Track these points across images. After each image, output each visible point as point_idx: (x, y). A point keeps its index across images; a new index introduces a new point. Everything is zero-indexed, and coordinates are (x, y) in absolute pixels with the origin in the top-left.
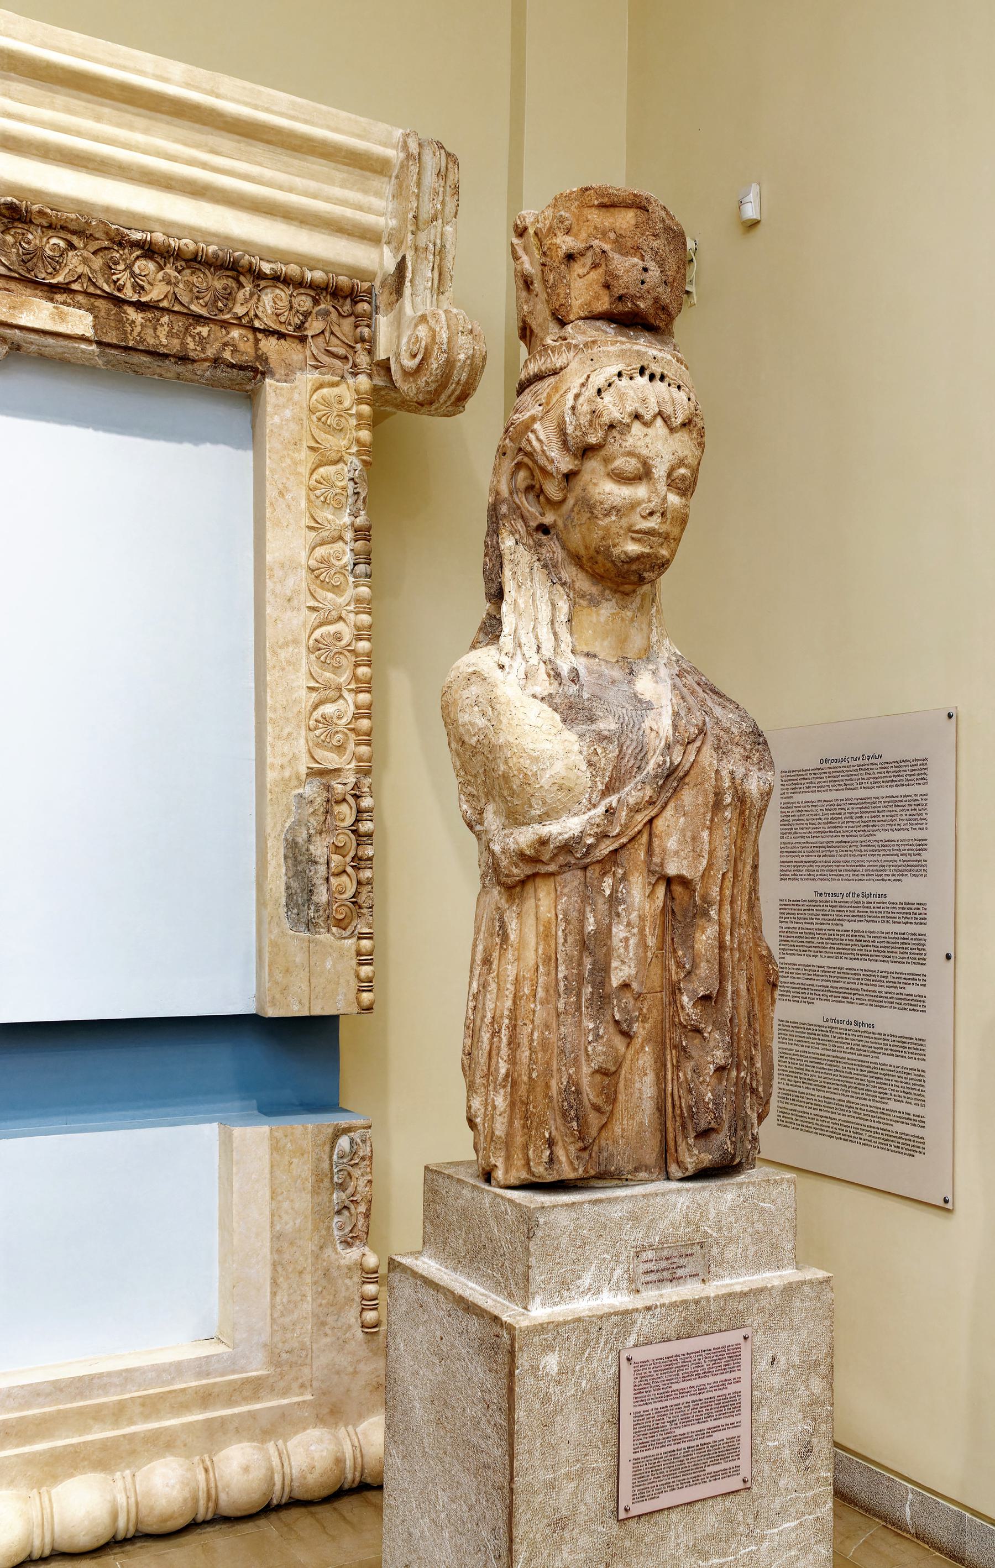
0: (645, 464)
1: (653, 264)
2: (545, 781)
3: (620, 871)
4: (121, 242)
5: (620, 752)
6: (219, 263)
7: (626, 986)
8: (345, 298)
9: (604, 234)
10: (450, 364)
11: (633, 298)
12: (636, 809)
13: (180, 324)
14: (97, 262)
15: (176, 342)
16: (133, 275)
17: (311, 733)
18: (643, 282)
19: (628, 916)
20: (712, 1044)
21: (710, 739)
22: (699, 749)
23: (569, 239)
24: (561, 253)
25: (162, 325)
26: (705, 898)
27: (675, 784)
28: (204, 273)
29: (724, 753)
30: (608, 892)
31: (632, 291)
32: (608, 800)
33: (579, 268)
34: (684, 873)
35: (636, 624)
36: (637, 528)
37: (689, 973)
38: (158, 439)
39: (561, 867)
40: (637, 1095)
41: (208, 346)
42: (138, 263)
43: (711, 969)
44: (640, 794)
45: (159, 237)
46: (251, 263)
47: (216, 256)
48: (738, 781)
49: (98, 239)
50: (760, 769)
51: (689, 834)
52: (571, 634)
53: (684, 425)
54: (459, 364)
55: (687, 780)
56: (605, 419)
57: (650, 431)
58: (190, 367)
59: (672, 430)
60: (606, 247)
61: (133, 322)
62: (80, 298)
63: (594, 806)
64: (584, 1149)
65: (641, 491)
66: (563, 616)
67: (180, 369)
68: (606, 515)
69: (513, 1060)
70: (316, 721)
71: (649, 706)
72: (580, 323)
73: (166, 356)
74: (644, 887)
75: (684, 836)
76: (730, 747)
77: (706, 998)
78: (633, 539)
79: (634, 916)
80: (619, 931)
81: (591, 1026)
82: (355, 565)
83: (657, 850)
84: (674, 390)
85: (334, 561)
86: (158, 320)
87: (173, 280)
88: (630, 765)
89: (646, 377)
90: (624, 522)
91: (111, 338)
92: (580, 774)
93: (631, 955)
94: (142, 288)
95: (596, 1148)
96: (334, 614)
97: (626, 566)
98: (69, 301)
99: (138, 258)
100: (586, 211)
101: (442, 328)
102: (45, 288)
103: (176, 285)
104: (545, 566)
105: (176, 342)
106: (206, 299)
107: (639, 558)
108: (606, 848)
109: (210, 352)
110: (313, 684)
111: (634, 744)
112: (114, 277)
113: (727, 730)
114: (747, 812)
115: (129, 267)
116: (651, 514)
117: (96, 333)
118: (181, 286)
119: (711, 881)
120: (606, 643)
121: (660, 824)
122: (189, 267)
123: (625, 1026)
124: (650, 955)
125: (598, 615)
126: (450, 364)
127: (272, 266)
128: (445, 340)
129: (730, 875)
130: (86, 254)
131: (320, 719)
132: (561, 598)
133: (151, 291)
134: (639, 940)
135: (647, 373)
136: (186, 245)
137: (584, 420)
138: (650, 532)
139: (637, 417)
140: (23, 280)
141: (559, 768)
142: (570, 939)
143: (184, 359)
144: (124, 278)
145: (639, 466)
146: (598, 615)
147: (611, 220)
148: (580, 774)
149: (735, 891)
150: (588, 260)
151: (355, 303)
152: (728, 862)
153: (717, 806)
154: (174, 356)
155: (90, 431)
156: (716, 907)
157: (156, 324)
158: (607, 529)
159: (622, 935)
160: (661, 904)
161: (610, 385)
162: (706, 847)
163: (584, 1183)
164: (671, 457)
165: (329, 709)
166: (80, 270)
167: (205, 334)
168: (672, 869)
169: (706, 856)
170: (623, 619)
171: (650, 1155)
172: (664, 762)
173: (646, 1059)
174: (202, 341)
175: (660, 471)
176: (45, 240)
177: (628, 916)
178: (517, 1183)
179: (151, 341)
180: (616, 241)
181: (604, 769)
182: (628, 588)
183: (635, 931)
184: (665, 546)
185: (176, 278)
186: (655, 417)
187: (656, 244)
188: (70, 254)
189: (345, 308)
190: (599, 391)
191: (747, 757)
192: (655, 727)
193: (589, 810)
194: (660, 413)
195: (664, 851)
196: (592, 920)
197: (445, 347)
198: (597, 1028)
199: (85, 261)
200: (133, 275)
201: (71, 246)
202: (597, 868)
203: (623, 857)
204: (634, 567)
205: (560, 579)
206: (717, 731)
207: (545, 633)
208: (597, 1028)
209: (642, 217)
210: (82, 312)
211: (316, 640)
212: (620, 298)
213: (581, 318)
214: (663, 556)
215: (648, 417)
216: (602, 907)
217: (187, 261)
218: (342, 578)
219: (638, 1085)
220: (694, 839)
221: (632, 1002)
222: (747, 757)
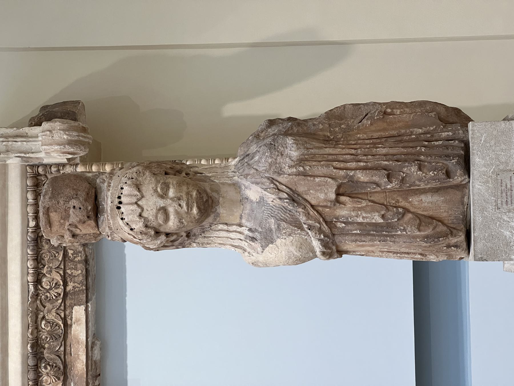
0: (159, 210)
1: (70, 203)
2: (298, 254)
3: (334, 220)
4: (36, 295)
5: (284, 221)
6: (36, 248)
7: (383, 217)
8: (37, 179)
9: (62, 224)
10: (70, 143)
11: (88, 212)
12: (308, 215)
13: (70, 265)
14: (48, 305)
15: (79, 266)
16: (51, 289)
18: (80, 208)
19: (353, 217)
20: (408, 172)
21: (275, 177)
22: (280, 183)
23: (66, 237)
24: (73, 239)
25: (72, 273)
26: (345, 178)
27: (296, 195)
28: (42, 254)
29: (281, 170)
30: (344, 225)
31: (85, 213)
32: (306, 229)
33: (78, 232)
34: (334, 190)
35: (225, 195)
36: (186, 210)
37: (378, 185)
38: (125, 266)
39: (333, 245)
40: (430, 205)
41: (78, 250)
42: (44, 286)
43: (376, 175)
44: (301, 213)
45: (30, 278)
46: (32, 232)
47: (32, 250)
48: (293, 164)
49: (37, 306)
50: (287, 148)
51: (317, 188)
52: (233, 225)
53: (139, 190)
54: (69, 138)
55: (294, 189)
56: (144, 229)
57: (145, 208)
58: (89, 257)
59: (143, 197)
60: (67, 224)
61: (73, 287)
62: (67, 313)
63: (308, 233)
64: (451, 233)
65: (171, 210)
66: (225, 227)
67: (91, 262)
68: (183, 223)
69: (415, 254)
71: (262, 198)
72: (100, 230)
73: (87, 270)
74: (341, 208)
75: (318, 190)
76: (278, 165)
77: (389, 176)
78: (191, 211)
79: (353, 214)
80: (360, 220)
81: (399, 233)
83: (325, 204)
84: (123, 191)
86: (70, 275)
87: (49, 269)
88: (289, 216)
89: (120, 205)
90: (185, 216)
91: (83, 297)
92: (294, 240)
93: (370, 215)
94: (56, 284)
95: (452, 226)
97: (203, 211)
98: (69, 317)
99: (42, 287)
100: (53, 231)
101: (52, 148)
102: (66, 328)
103: (51, 268)
104: (204, 232)
105: (79, 266)
106: (55, 253)
107: (198, 207)
108: (325, 228)
109: (81, 249)
111: (280, 212)
112: (54, 298)
113: (270, 165)
114: (306, 157)
115: (48, 291)
116: (180, 205)
117: (82, 305)
118: (51, 265)
119: (337, 175)
120: (235, 210)
121: (313, 202)
122: (41, 261)
123: (400, 216)
124: (370, 204)
125: (223, 213)
126: (70, 143)
127: (30, 220)
128: (59, 147)
129: (335, 164)
130: (45, 311)
132: (217, 227)
133: (56, 279)
134: (364, 210)
135: (119, 205)
136: (31, 265)
137: (145, 237)
138: (188, 205)
139: (140, 215)
140: (65, 339)
141: (293, 249)
142: (363, 239)
143: (86, 261)
144: (53, 293)
145: (160, 212)
146: (223, 213)
147: (56, 222)
148: (294, 240)
149: (341, 159)
150: (74, 229)
151: (39, 175)
152: (328, 166)
153: (305, 174)
154: (86, 266)
155: (127, 298)
156: (349, 172)
157: (72, 276)
158: (188, 222)
159: (361, 219)
160: (348, 198)
161: (128, 224)
162: (323, 178)
163: (468, 224)
164: (154, 197)
166: (55, 314)
167: (72, 252)
168: (333, 196)
169: (327, 178)
170: (224, 203)
171: (456, 195)
172: (287, 202)
173: (415, 200)
174: (76, 253)
175: (161, 203)
176: (44, 331)
177: (353, 217)
178: (467, 252)
179: (81, 278)
180: (64, 219)
181: (292, 229)
182: (210, 201)
183: (359, 213)
184: (191, 193)
185: (47, 268)
186: (139, 206)
187: (62, 202)
188: (47, 318)
189: (43, 179)
190: (132, 229)
191: (282, 155)
192: (272, 200)
193: (309, 235)
194: (136, 203)
195: (325, 200)
196: (355, 232)
197: (62, 147)
198: (401, 231)
199: (49, 311)
200: (51, 289)
201: (44, 318)
202: (333, 230)
203: (328, 219)
204: (203, 207)
205: (209, 227)
206: (271, 172)
207: (232, 235)
208: (400, 229)
209: (52, 210)
210: (73, 311)
212: (88, 217)
213: (98, 230)
214: (196, 194)
215: (140, 210)
216: (349, 227)
217: (38, 263)
219: (426, 204)
220: (319, 186)
221: (390, 212)
222: (282, 155)
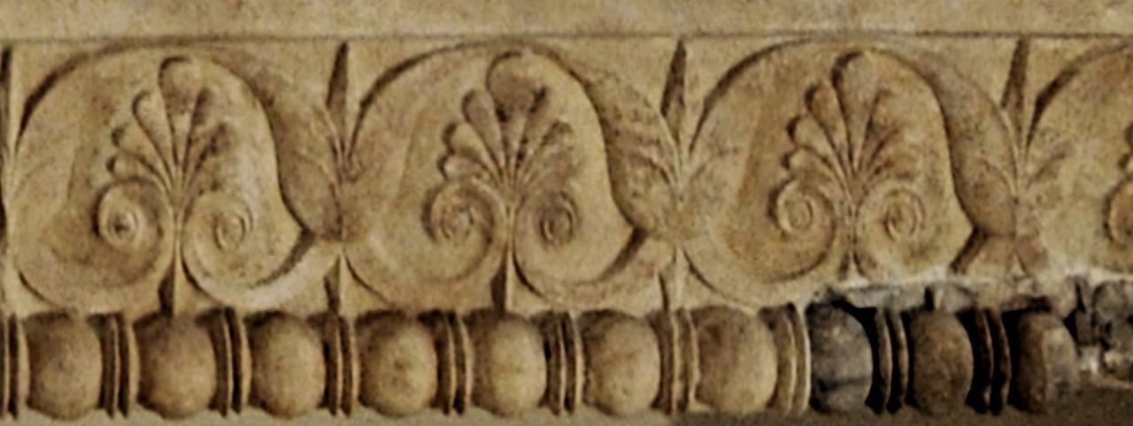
17: (144, 65)
70: (203, 99)
82: (866, 316)
85: (879, 195)
96: (652, 202)
110: (359, 83)
131: (211, 124)
165: (252, 166)
211: (541, 96)
218: (809, 242)
